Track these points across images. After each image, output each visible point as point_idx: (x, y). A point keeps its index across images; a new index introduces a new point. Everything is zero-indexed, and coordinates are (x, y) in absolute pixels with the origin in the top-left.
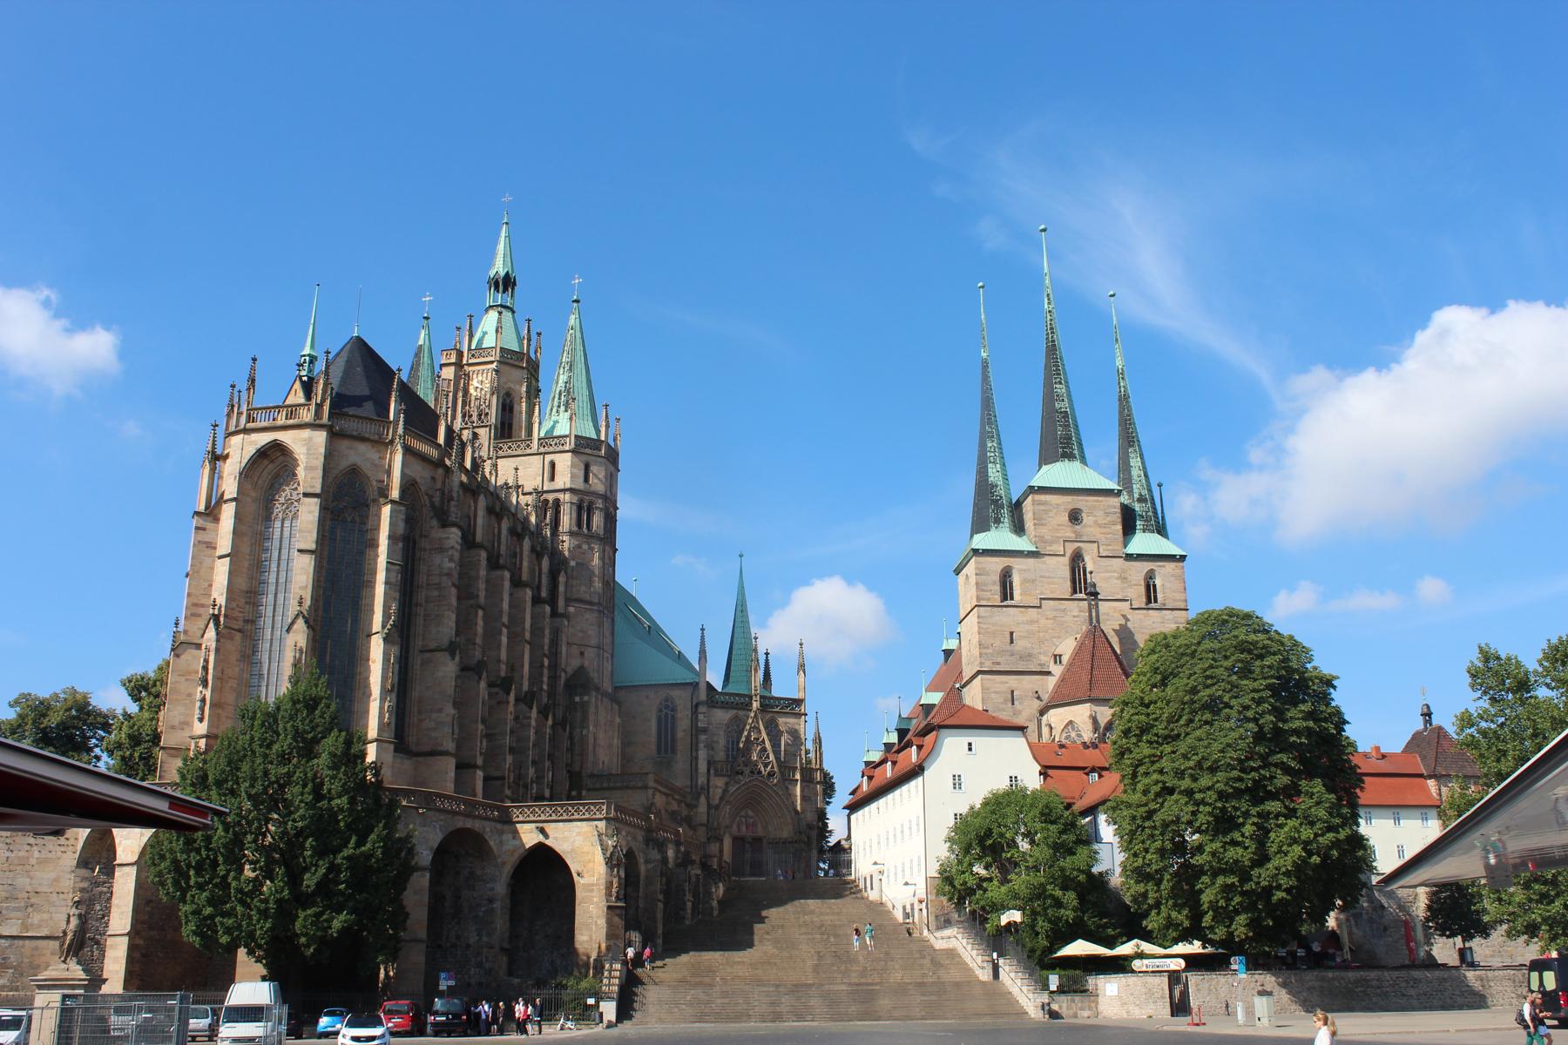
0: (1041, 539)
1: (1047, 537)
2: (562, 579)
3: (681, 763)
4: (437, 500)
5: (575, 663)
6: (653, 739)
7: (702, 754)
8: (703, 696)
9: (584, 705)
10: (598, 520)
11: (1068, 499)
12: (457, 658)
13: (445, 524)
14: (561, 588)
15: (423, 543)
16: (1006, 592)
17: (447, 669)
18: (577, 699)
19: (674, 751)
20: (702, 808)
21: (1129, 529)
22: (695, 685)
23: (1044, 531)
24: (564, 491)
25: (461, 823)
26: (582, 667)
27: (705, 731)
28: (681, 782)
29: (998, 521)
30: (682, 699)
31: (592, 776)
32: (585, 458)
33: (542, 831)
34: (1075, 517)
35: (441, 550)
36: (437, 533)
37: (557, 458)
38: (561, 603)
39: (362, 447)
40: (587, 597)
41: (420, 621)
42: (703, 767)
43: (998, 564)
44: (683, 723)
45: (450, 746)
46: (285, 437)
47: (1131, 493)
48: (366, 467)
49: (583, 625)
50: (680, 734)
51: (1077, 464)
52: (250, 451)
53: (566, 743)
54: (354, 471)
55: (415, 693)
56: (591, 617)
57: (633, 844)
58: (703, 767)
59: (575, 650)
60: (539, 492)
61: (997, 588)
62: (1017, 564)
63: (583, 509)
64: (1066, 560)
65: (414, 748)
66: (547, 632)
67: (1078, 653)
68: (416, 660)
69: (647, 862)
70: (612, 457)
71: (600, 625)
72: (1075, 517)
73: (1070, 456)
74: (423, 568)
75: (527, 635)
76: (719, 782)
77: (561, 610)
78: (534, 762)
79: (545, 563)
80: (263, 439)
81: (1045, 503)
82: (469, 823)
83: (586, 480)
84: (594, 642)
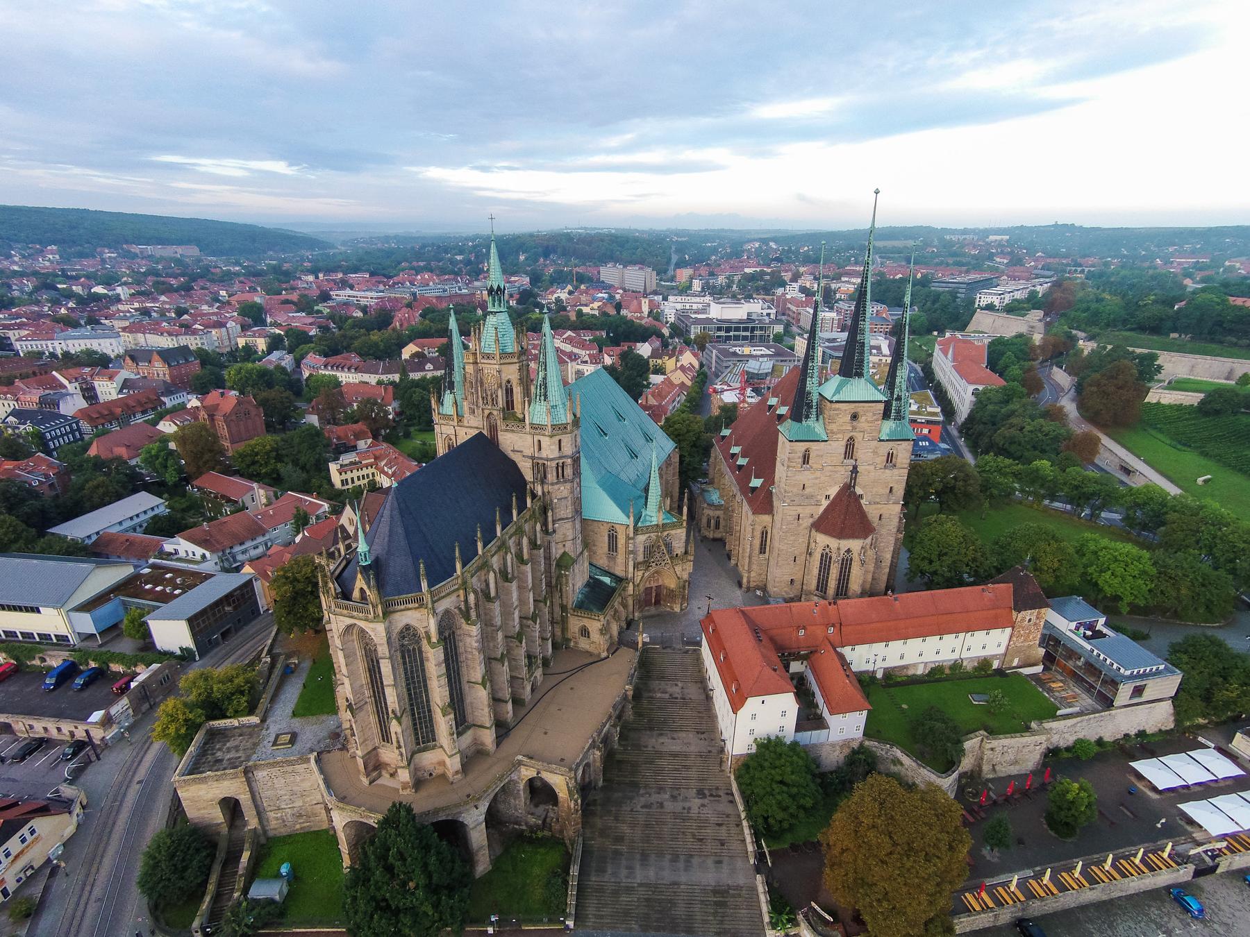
2: (550, 514)
5: (561, 552)
10: (569, 471)
14: (550, 519)
16: (806, 459)
21: (886, 415)
26: (565, 553)
29: (807, 417)
34: (855, 417)
37: (541, 438)
38: (550, 526)
43: (801, 447)
47: (892, 393)
53: (557, 595)
56: (569, 525)
59: (560, 545)
60: (533, 458)
61: (801, 460)
62: (813, 446)
63: (560, 468)
64: (844, 443)
67: (838, 494)
72: (855, 417)
73: (860, 375)
77: (551, 530)
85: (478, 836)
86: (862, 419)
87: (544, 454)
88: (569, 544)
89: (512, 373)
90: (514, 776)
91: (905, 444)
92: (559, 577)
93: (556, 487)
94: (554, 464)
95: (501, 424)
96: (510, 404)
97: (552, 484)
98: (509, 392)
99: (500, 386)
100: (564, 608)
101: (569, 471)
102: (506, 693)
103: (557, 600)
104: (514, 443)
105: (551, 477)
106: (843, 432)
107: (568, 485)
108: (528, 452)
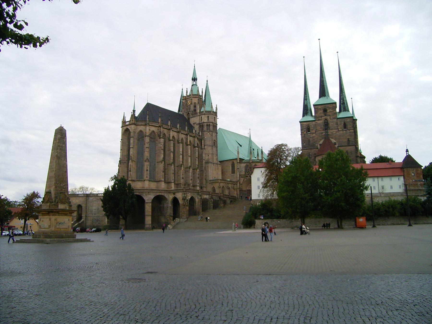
0: (315, 117)
1: (317, 116)
2: (203, 141)
4: (159, 134)
5: (207, 158)
8: (238, 161)
9: (208, 166)
10: (211, 127)
11: (323, 106)
12: (163, 163)
13: (160, 138)
14: (203, 143)
15: (157, 142)
16: (308, 130)
17: (161, 166)
20: (238, 185)
22: (237, 159)
23: (317, 115)
24: (204, 123)
25: (158, 194)
27: (238, 169)
28: (235, 180)
30: (235, 162)
31: (210, 181)
32: (207, 115)
33: (174, 194)
34: (325, 111)
35: (160, 143)
36: (159, 140)
37: (202, 116)
38: (203, 146)
39: (142, 126)
40: (209, 144)
41: (157, 157)
44: (236, 167)
45: (163, 180)
46: (128, 127)
48: (143, 130)
49: (208, 150)
51: (326, 97)
52: (124, 130)
54: (141, 131)
55: (156, 170)
56: (210, 148)
57: (192, 195)
58: (238, 176)
60: (199, 124)
62: (311, 124)
66: (197, 153)
68: (157, 164)
69: (198, 198)
70: (215, 114)
71: (212, 149)
74: (157, 147)
75: (190, 155)
77: (203, 148)
78: (191, 180)
79: (196, 139)
80: (125, 128)
81: (317, 108)
82: (160, 194)
83: (208, 120)
85: (148, 208)
87: (203, 122)
88: (210, 155)
89: (195, 100)
90: (166, 195)
91: (349, 120)
92: (205, 168)
93: (206, 133)
94: (206, 124)
95: (191, 116)
96: (195, 110)
97: (205, 131)
98: (195, 106)
99: (191, 103)
100: (206, 180)
101: (211, 127)
102: (172, 179)
103: (204, 177)
104: (194, 120)
105: (205, 128)
106: (321, 117)
107: (211, 133)
108: (198, 122)
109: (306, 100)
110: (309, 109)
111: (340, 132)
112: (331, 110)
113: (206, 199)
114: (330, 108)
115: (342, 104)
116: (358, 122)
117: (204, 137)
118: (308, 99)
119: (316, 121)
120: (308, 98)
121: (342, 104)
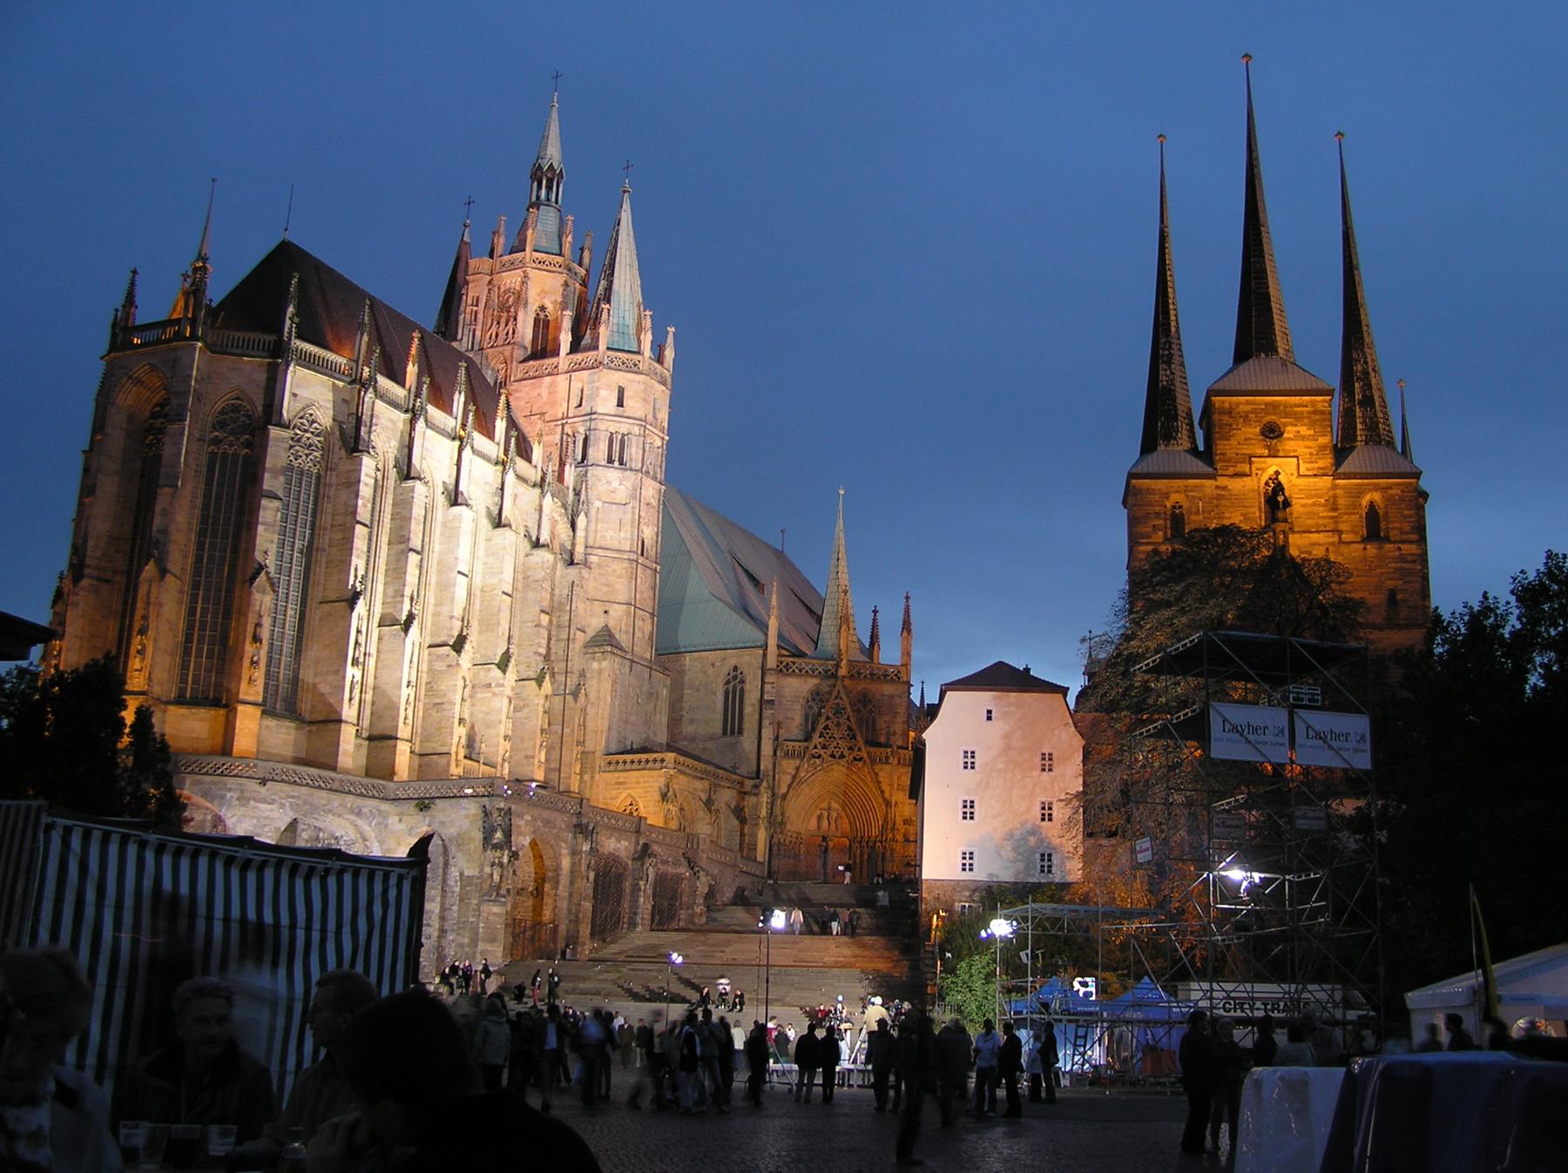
2: (581, 521)
3: (747, 742)
6: (719, 716)
7: (767, 733)
18: (595, 665)
19: (740, 732)
40: (616, 545)
42: (767, 748)
50: (748, 710)
58: (767, 748)
59: (598, 608)
65: (307, 717)
74: (328, 507)
76: (789, 766)
83: (620, 404)
84: (622, 598)
86: (1290, 432)
105: (598, 452)
109: (1169, 362)
110: (1181, 413)
111: (1344, 549)
112: (1304, 430)
113: (614, 859)
114: (1298, 418)
115: (1361, 403)
116: (1429, 508)
117: (588, 502)
118: (1176, 360)
119: (1222, 481)
120: (1175, 352)
121: (1361, 403)
